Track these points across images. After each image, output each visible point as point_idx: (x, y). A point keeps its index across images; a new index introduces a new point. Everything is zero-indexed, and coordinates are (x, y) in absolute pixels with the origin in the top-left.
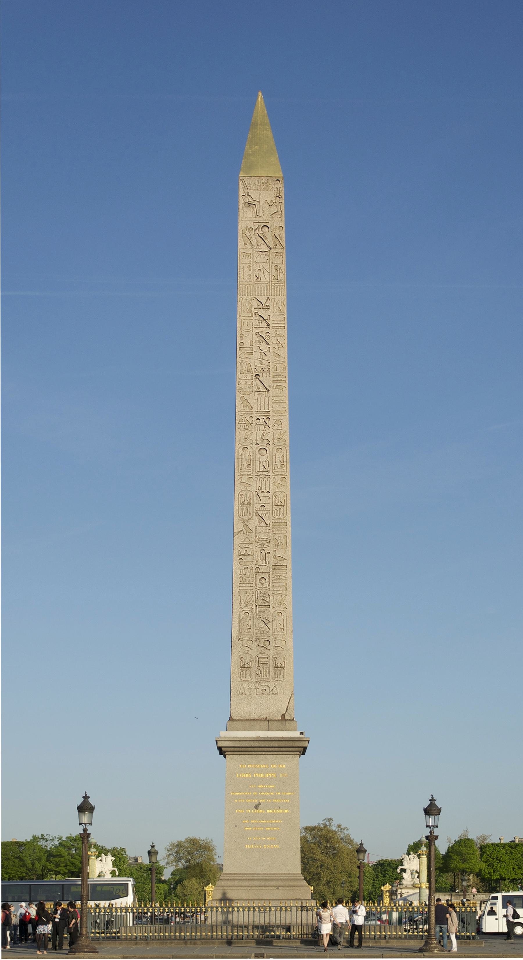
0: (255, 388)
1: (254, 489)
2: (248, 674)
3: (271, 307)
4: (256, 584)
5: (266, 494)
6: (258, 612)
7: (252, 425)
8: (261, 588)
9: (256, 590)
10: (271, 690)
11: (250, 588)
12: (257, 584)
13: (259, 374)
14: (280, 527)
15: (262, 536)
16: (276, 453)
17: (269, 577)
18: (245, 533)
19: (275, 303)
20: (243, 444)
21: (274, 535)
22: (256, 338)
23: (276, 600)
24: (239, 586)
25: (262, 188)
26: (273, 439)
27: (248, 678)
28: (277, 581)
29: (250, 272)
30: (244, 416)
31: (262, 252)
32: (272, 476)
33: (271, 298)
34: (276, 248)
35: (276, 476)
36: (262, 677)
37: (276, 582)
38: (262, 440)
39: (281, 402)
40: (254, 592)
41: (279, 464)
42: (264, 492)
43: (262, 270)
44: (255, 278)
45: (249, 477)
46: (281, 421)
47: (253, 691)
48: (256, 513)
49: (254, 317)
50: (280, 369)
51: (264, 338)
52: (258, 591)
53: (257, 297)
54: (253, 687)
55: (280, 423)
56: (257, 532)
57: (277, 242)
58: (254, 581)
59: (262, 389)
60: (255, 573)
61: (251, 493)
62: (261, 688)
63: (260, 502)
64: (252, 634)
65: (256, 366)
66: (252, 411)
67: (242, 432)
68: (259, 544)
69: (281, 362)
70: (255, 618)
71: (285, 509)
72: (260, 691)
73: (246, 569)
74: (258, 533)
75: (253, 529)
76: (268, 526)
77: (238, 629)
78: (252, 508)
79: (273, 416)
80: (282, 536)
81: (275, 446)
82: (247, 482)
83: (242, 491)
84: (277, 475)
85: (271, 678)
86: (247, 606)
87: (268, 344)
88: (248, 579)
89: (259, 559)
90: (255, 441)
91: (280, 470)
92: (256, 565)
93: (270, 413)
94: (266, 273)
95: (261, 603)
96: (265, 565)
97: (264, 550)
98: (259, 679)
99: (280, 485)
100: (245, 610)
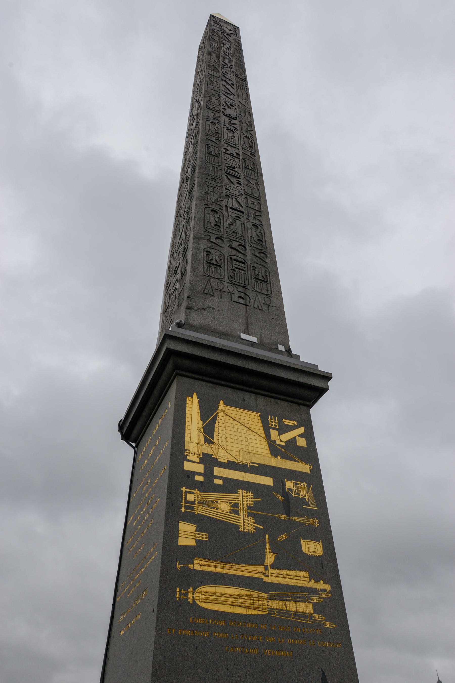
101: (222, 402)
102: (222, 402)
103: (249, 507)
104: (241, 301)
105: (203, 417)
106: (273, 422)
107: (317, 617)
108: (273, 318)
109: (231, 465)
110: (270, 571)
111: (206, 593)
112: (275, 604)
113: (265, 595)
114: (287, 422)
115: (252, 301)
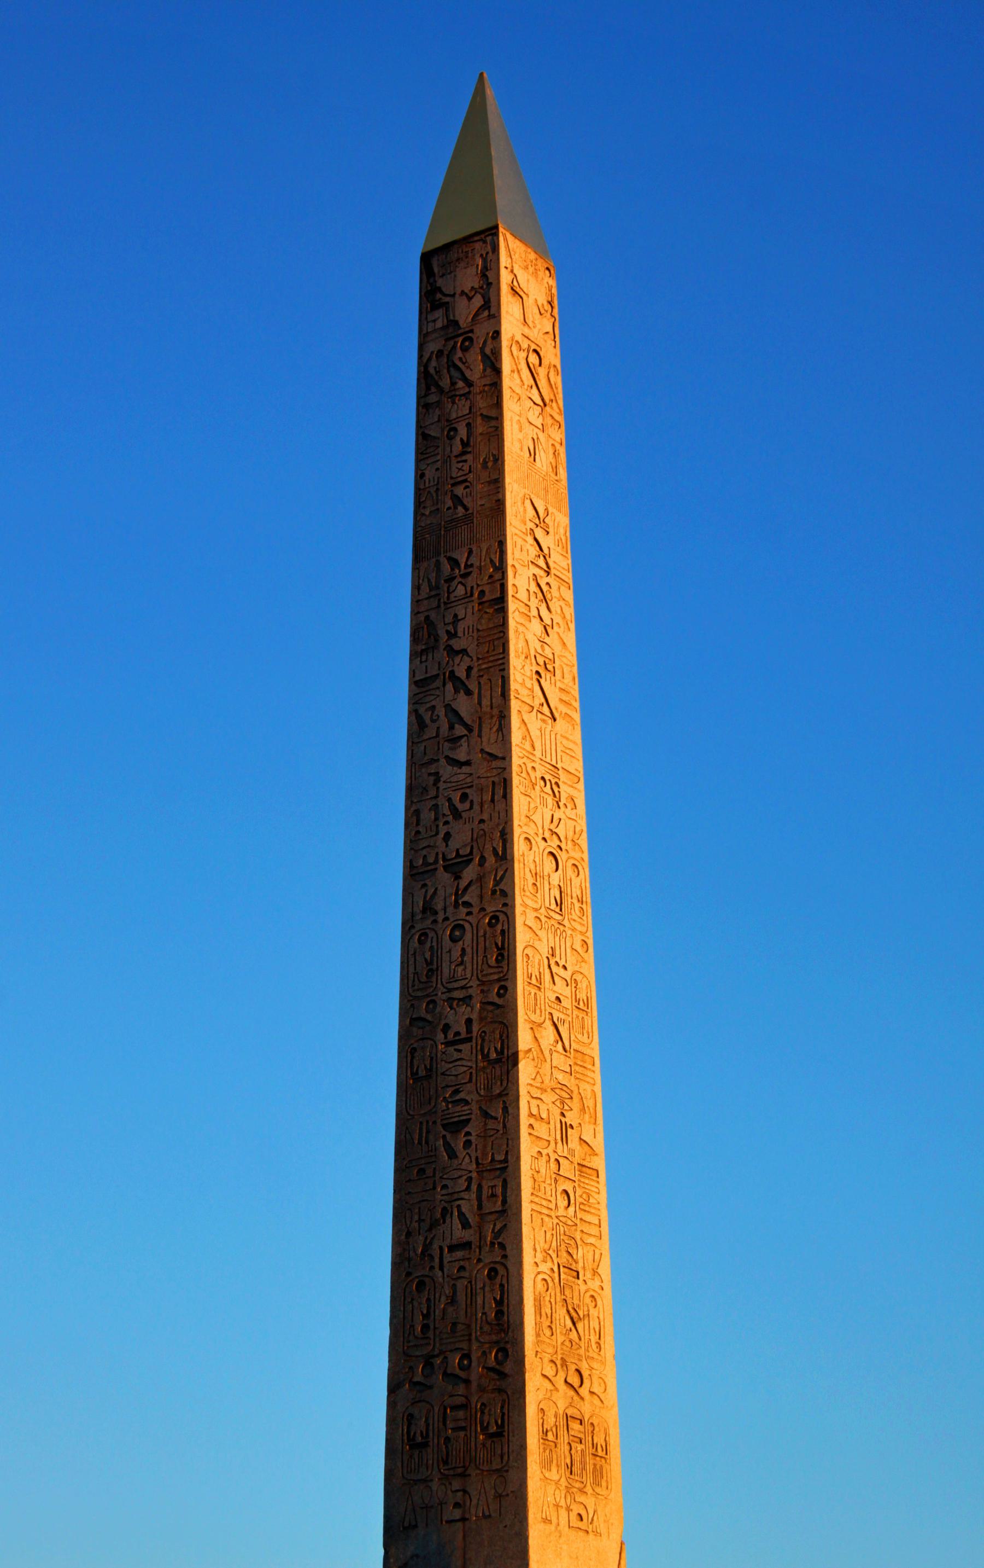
0: (536, 704)
1: (545, 952)
2: (555, 1462)
3: (551, 530)
4: (556, 1204)
5: (561, 972)
6: (562, 1284)
14: (585, 1065)
15: (560, 1077)
17: (575, 1193)
19: (556, 525)
21: (577, 1081)
22: (533, 588)
23: (587, 1262)
28: (587, 1209)
33: (550, 510)
36: (576, 1478)
39: (574, 755)
40: (555, 1227)
41: (577, 905)
44: (528, 455)
46: (575, 799)
49: (530, 540)
52: (561, 1224)
53: (532, 496)
54: (563, 1503)
56: (554, 1065)
61: (540, 958)
62: (576, 1509)
63: (555, 988)
66: (534, 755)
68: (557, 1097)
70: (558, 1299)
78: (543, 997)
80: (588, 1088)
84: (574, 930)
85: (588, 1484)
86: (544, 1261)
89: (559, 1137)
90: (541, 831)
93: (559, 772)
95: (565, 1260)
98: (570, 1481)
104: (457, 1514)
108: (505, 1526)
115: (474, 1502)
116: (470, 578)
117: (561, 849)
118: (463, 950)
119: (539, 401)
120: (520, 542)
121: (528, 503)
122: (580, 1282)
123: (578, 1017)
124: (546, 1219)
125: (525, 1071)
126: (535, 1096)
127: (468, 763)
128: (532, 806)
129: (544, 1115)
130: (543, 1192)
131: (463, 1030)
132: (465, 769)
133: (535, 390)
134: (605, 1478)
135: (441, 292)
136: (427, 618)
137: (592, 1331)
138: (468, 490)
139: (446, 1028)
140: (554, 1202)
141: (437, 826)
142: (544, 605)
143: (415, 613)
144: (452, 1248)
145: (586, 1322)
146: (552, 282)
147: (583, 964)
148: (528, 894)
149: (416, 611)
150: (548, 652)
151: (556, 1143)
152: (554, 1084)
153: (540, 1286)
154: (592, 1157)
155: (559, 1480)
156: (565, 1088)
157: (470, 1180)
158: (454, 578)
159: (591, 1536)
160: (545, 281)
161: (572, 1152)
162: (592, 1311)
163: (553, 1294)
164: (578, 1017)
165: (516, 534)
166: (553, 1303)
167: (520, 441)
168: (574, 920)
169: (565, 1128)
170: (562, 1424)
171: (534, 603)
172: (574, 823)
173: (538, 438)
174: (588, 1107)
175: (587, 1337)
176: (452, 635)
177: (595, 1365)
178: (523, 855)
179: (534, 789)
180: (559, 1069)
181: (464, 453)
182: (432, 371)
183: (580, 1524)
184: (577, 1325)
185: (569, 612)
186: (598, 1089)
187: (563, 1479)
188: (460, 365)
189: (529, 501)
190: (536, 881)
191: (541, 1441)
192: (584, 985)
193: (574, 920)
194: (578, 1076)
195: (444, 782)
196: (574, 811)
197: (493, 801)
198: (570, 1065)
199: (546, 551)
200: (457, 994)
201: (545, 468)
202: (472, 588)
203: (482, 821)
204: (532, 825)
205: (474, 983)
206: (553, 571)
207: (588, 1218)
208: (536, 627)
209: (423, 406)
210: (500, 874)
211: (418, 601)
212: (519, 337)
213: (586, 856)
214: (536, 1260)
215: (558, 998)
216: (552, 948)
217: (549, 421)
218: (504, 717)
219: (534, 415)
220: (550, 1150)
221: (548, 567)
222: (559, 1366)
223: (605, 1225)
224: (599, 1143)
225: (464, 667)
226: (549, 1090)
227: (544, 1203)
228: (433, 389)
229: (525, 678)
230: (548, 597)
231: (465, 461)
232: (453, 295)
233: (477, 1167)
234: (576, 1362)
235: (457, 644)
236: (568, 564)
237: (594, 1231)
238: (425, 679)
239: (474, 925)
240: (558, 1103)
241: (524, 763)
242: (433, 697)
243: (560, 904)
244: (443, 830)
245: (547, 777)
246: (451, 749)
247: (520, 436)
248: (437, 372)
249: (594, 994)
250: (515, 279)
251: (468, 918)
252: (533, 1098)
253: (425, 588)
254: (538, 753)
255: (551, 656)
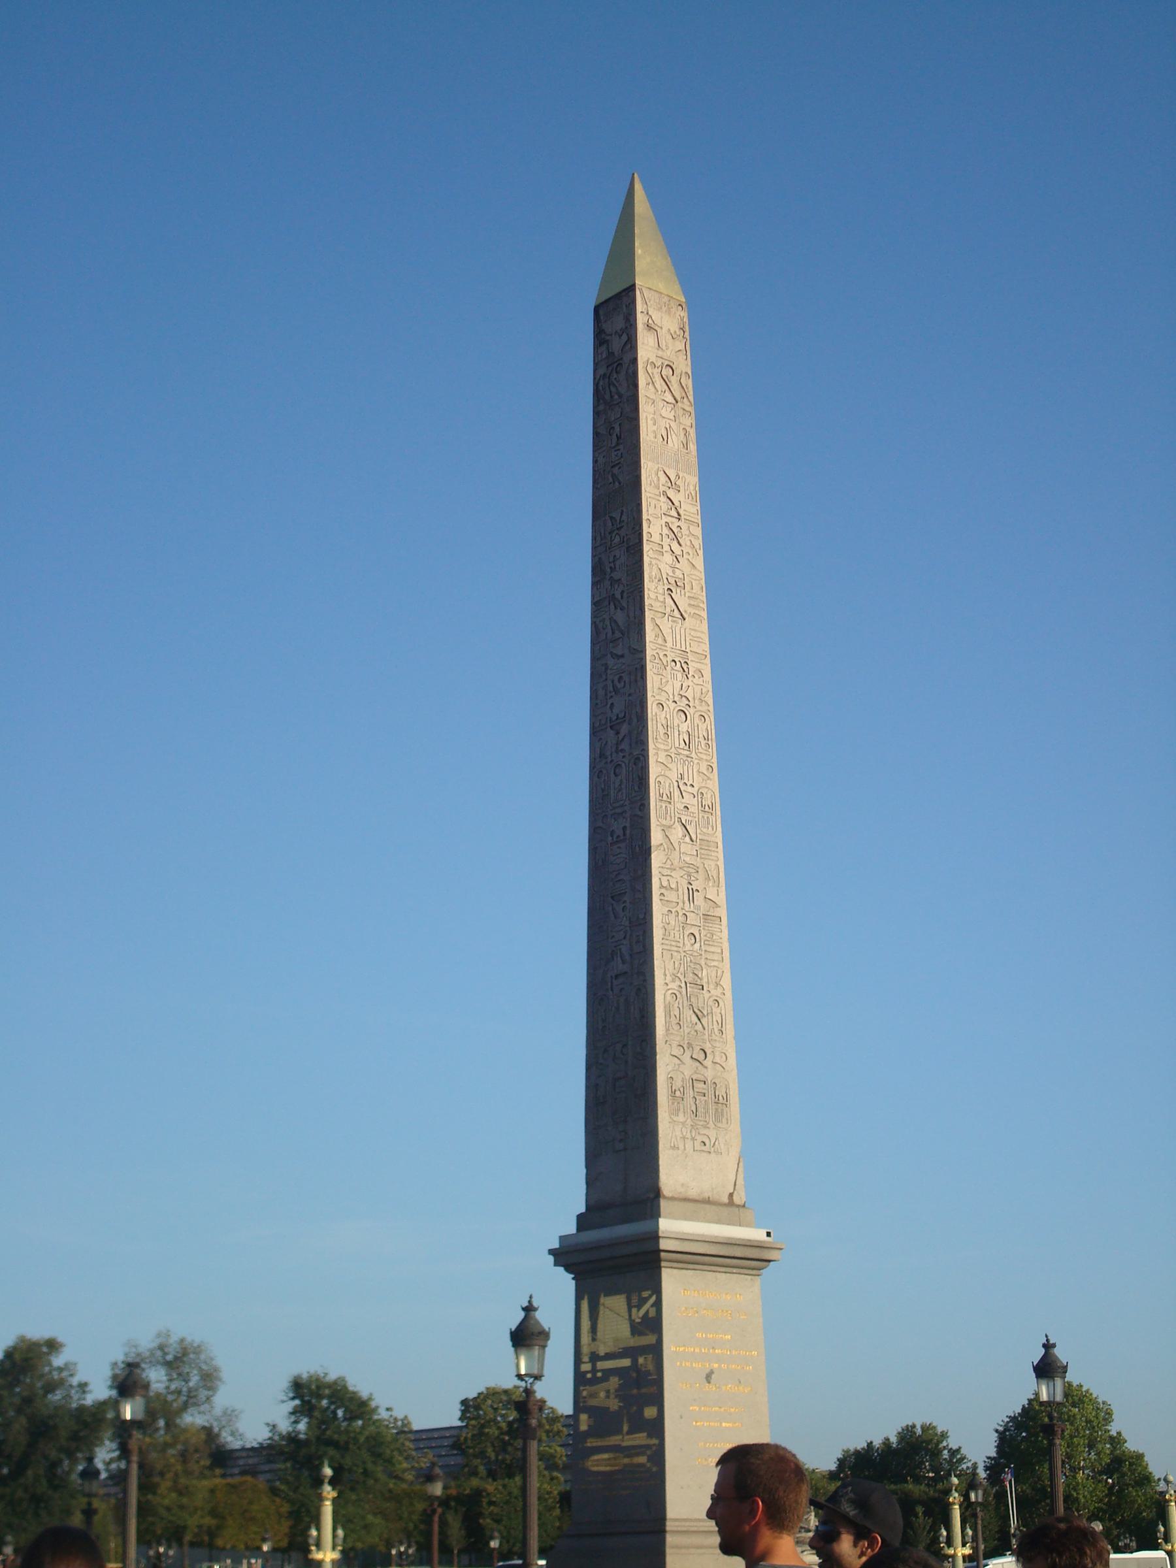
0: (668, 610)
1: (674, 776)
2: (682, 1110)
3: (682, 489)
5: (690, 789)
7: (667, 668)
8: (690, 952)
9: (685, 954)
10: (712, 1145)
11: (676, 949)
12: (686, 943)
13: (672, 588)
14: (710, 848)
15: (687, 859)
16: (698, 722)
17: (700, 934)
18: (667, 850)
19: (686, 484)
20: (657, 697)
21: (702, 860)
22: (666, 531)
24: (662, 944)
25: (664, 309)
26: (694, 698)
27: (681, 1118)
28: (711, 943)
29: (655, 428)
30: (656, 651)
31: (667, 403)
32: (696, 759)
34: (683, 403)
35: (699, 760)
36: (700, 1118)
37: (709, 945)
38: (680, 696)
39: (701, 640)
40: (682, 958)
41: (703, 742)
42: (686, 785)
43: (669, 429)
44: (662, 439)
45: (666, 753)
46: (702, 671)
47: (689, 1144)
48: (678, 818)
49: (663, 499)
50: (696, 588)
51: (676, 533)
52: (688, 956)
54: (689, 1135)
55: (701, 676)
56: (682, 852)
57: (685, 396)
58: (682, 937)
59: (676, 613)
60: (683, 923)
62: (699, 1139)
63: (683, 801)
64: (682, 1034)
65: (668, 574)
66: (666, 646)
67: (655, 677)
68: (684, 872)
69: (698, 578)
70: (685, 1005)
71: (714, 819)
72: (698, 1146)
73: (670, 914)
74: (683, 853)
75: (676, 845)
76: (695, 843)
77: (664, 1022)
78: (673, 808)
79: (692, 661)
80: (713, 864)
81: (696, 711)
82: (665, 763)
83: (659, 776)
84: (701, 759)
85: (711, 1122)
86: (673, 981)
87: (680, 545)
88: (673, 931)
90: (671, 697)
91: (705, 752)
92: (682, 909)
93: (688, 655)
94: (674, 436)
95: (691, 979)
96: (694, 912)
97: (691, 885)
99: (706, 778)
100: (672, 989)
101: (602, 1295)
102: (602, 1295)
103: (616, 1391)
105: (591, 1320)
106: (635, 1301)
107: (648, 1465)
109: (609, 1356)
110: (626, 1437)
111: (594, 1461)
112: (626, 1461)
113: (622, 1455)
114: (645, 1294)
116: (622, 530)
117: (690, 707)
118: (621, 781)
119: (671, 400)
120: (653, 502)
121: (661, 474)
122: (704, 992)
123: (703, 817)
124: (675, 954)
125: (657, 860)
126: (665, 874)
127: (622, 656)
128: (664, 681)
129: (673, 886)
130: (673, 936)
131: (620, 833)
132: (621, 660)
133: (668, 394)
134: (725, 1116)
135: (605, 333)
136: (600, 558)
137: (715, 1023)
138: (620, 470)
139: (612, 833)
140: (682, 941)
141: (607, 699)
142: (675, 542)
143: (593, 556)
144: (617, 977)
145: (710, 1017)
146: (684, 314)
147: (708, 781)
148: (660, 741)
149: (594, 554)
150: (678, 573)
151: (684, 903)
152: (681, 865)
153: (669, 998)
154: (715, 909)
155: (686, 1121)
156: (691, 866)
157: (626, 932)
158: (614, 531)
159: (713, 1155)
160: (678, 313)
161: (699, 908)
162: (714, 1010)
163: (681, 1002)
164: (703, 817)
165: (650, 497)
166: (681, 1009)
167: (654, 432)
168: (700, 753)
169: (691, 893)
170: (688, 1085)
171: (666, 542)
172: (700, 687)
173: (670, 427)
174: (712, 876)
175: (711, 1027)
176: (612, 569)
177: (717, 1044)
178: (656, 714)
179: (666, 669)
180: (686, 854)
181: (618, 444)
182: (601, 388)
183: (704, 1148)
184: (701, 1020)
185: (698, 543)
186: (721, 864)
187: (689, 1120)
188: (615, 382)
189: (662, 472)
190: (668, 731)
191: (670, 1097)
192: (709, 796)
193: (700, 753)
194: (703, 856)
195: (611, 669)
196: (702, 678)
197: (636, 681)
198: (697, 850)
199: (677, 504)
200: (619, 810)
201: (676, 446)
202: (624, 537)
203: (630, 695)
204: (663, 693)
205: (627, 803)
206: (683, 517)
207: (712, 949)
208: (668, 558)
209: (597, 414)
210: (641, 728)
211: (595, 547)
212: (653, 359)
213: (711, 708)
214: (666, 981)
215: (686, 807)
216: (681, 774)
217: (681, 412)
218: (642, 624)
219: (667, 412)
220: (678, 909)
221: (679, 515)
222: (685, 1048)
223: (726, 954)
224: (721, 899)
225: (620, 590)
226: (678, 869)
227: (674, 943)
228: (601, 401)
229: (658, 595)
230: (679, 535)
231: (619, 450)
232: (611, 335)
233: (630, 923)
234: (701, 1044)
235: (616, 576)
236: (698, 510)
237: (716, 957)
238: (600, 600)
239: (627, 764)
240: (686, 877)
241: (657, 653)
242: (603, 613)
243: (688, 744)
244: (610, 702)
245: (676, 660)
246: (613, 647)
247: (655, 428)
248: (603, 389)
249: (718, 800)
250: (650, 319)
251: (623, 760)
252: (663, 875)
253: (598, 538)
254: (669, 644)
255: (681, 576)
